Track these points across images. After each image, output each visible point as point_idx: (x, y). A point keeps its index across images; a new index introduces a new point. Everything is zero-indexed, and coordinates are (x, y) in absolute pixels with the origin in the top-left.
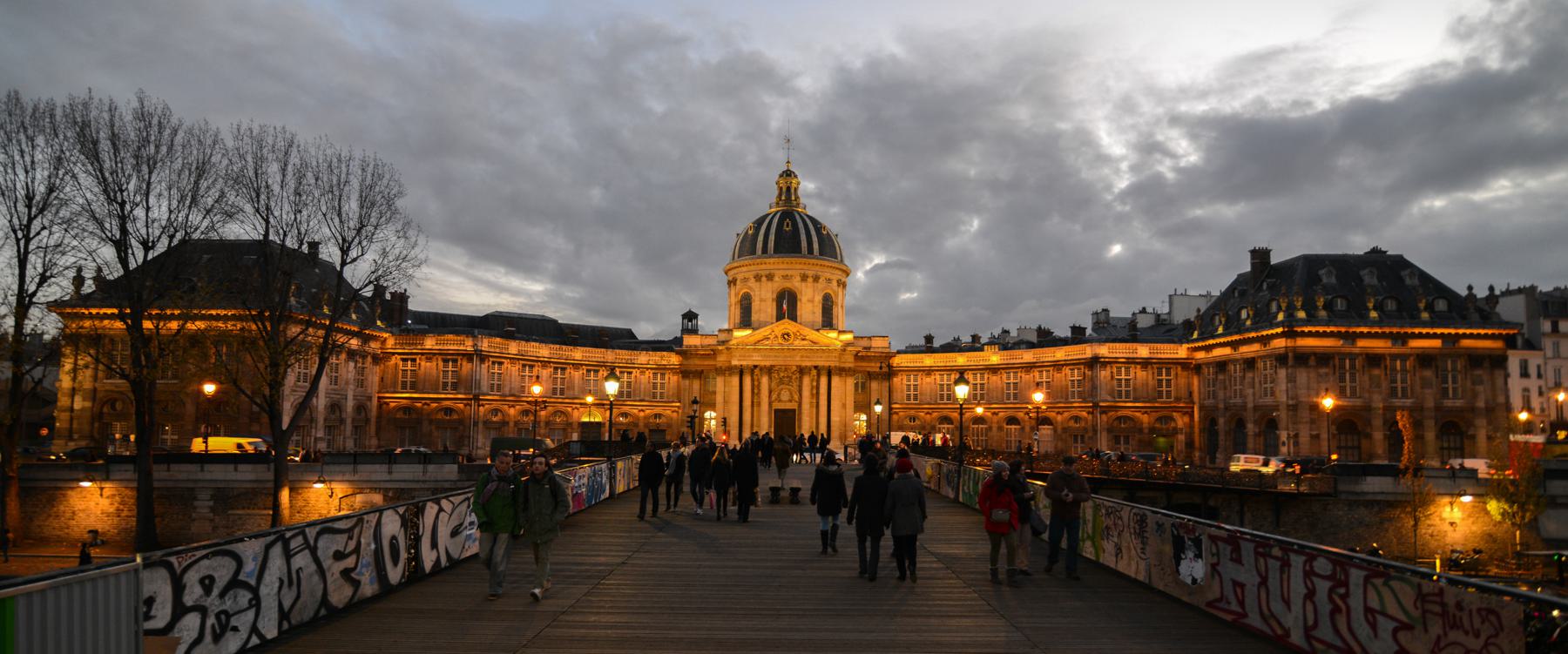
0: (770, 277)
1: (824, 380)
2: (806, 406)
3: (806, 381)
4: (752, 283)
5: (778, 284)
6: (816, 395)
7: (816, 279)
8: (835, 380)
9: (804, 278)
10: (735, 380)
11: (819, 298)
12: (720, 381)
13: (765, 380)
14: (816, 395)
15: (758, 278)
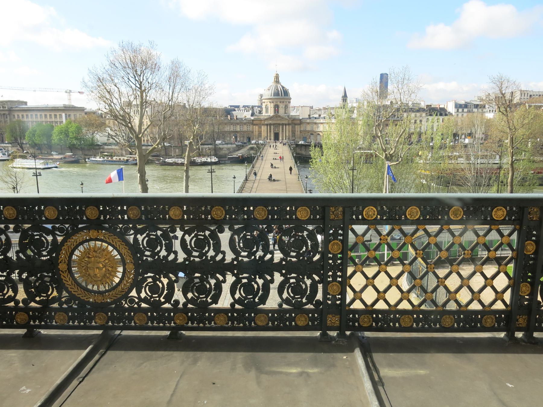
0: (273, 102)
1: (284, 127)
2: (281, 132)
3: (281, 127)
4: (269, 104)
5: (275, 103)
6: (283, 129)
7: (283, 102)
8: (287, 126)
9: (280, 102)
10: (266, 127)
11: (284, 106)
12: (263, 127)
13: (272, 127)
14: (283, 129)
15: (270, 102)
